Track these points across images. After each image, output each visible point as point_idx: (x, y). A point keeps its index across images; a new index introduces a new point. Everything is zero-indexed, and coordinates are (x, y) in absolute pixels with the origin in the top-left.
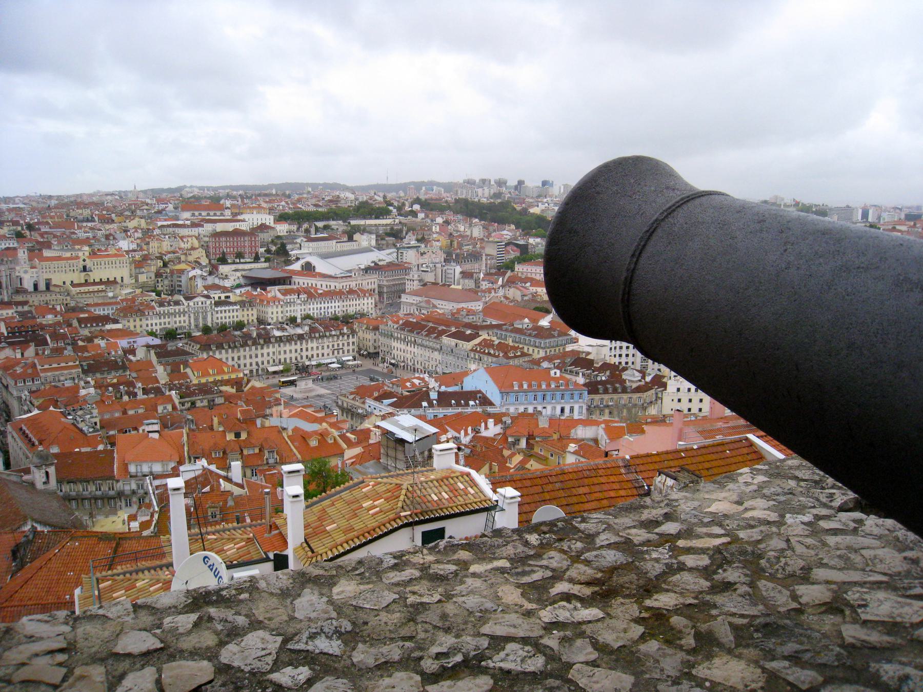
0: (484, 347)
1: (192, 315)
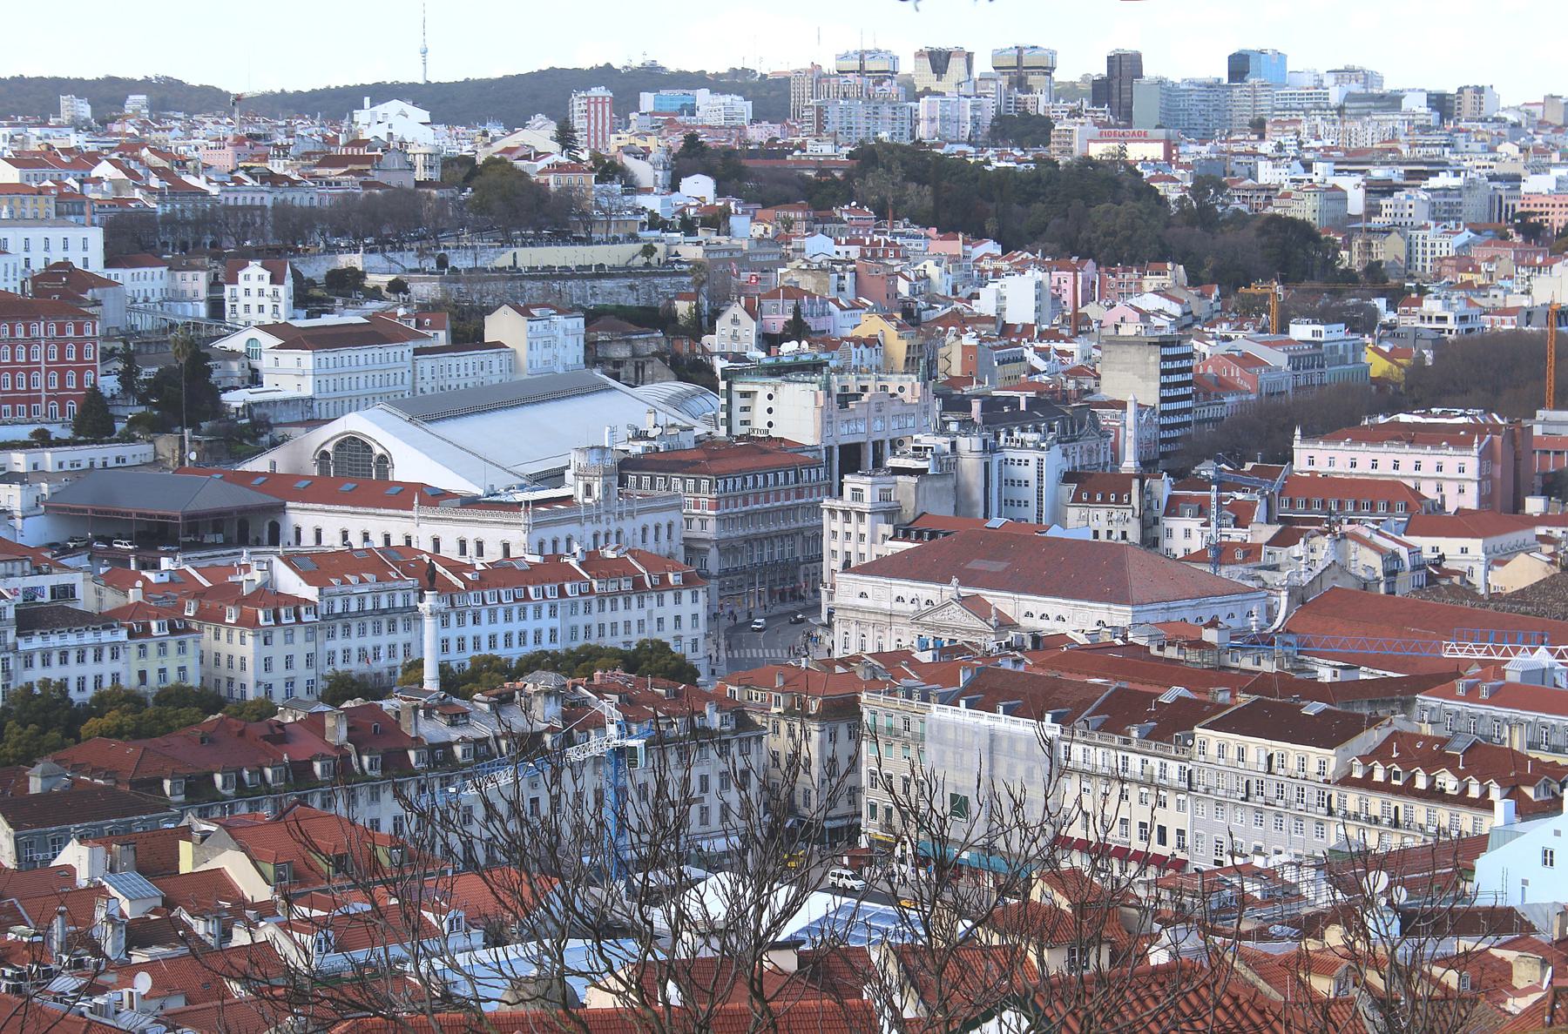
0: (1407, 762)
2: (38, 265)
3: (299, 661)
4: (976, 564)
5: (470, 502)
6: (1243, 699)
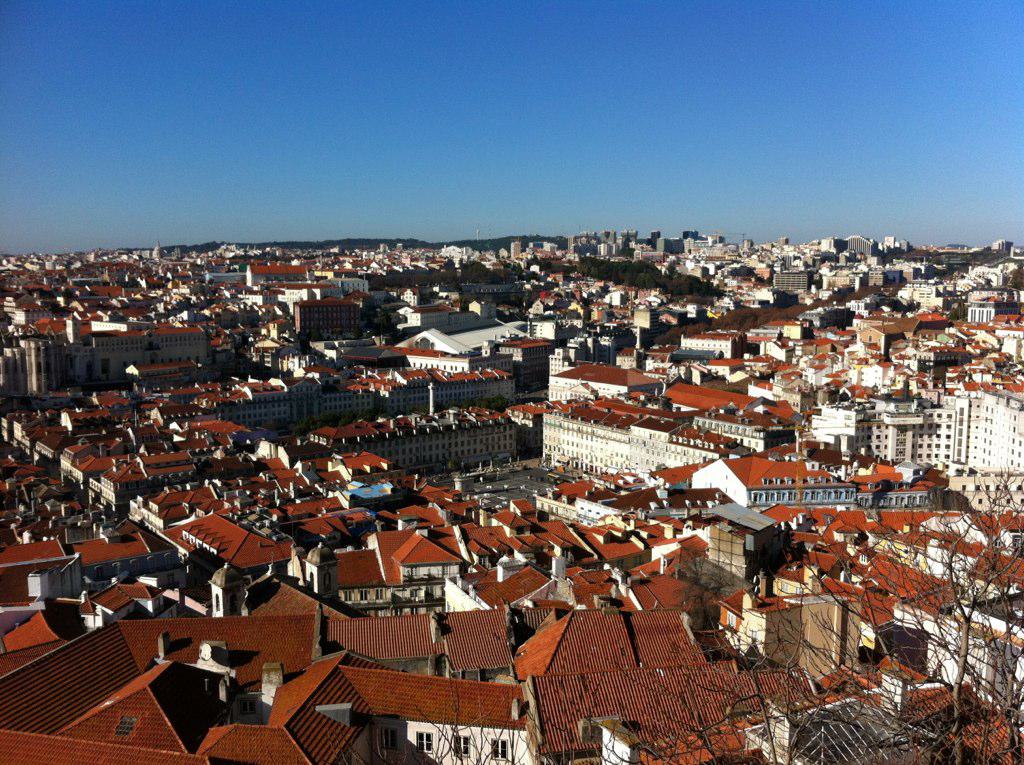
0: (688, 437)
1: (294, 405)
4: (587, 374)
5: (454, 356)
6: (648, 416)
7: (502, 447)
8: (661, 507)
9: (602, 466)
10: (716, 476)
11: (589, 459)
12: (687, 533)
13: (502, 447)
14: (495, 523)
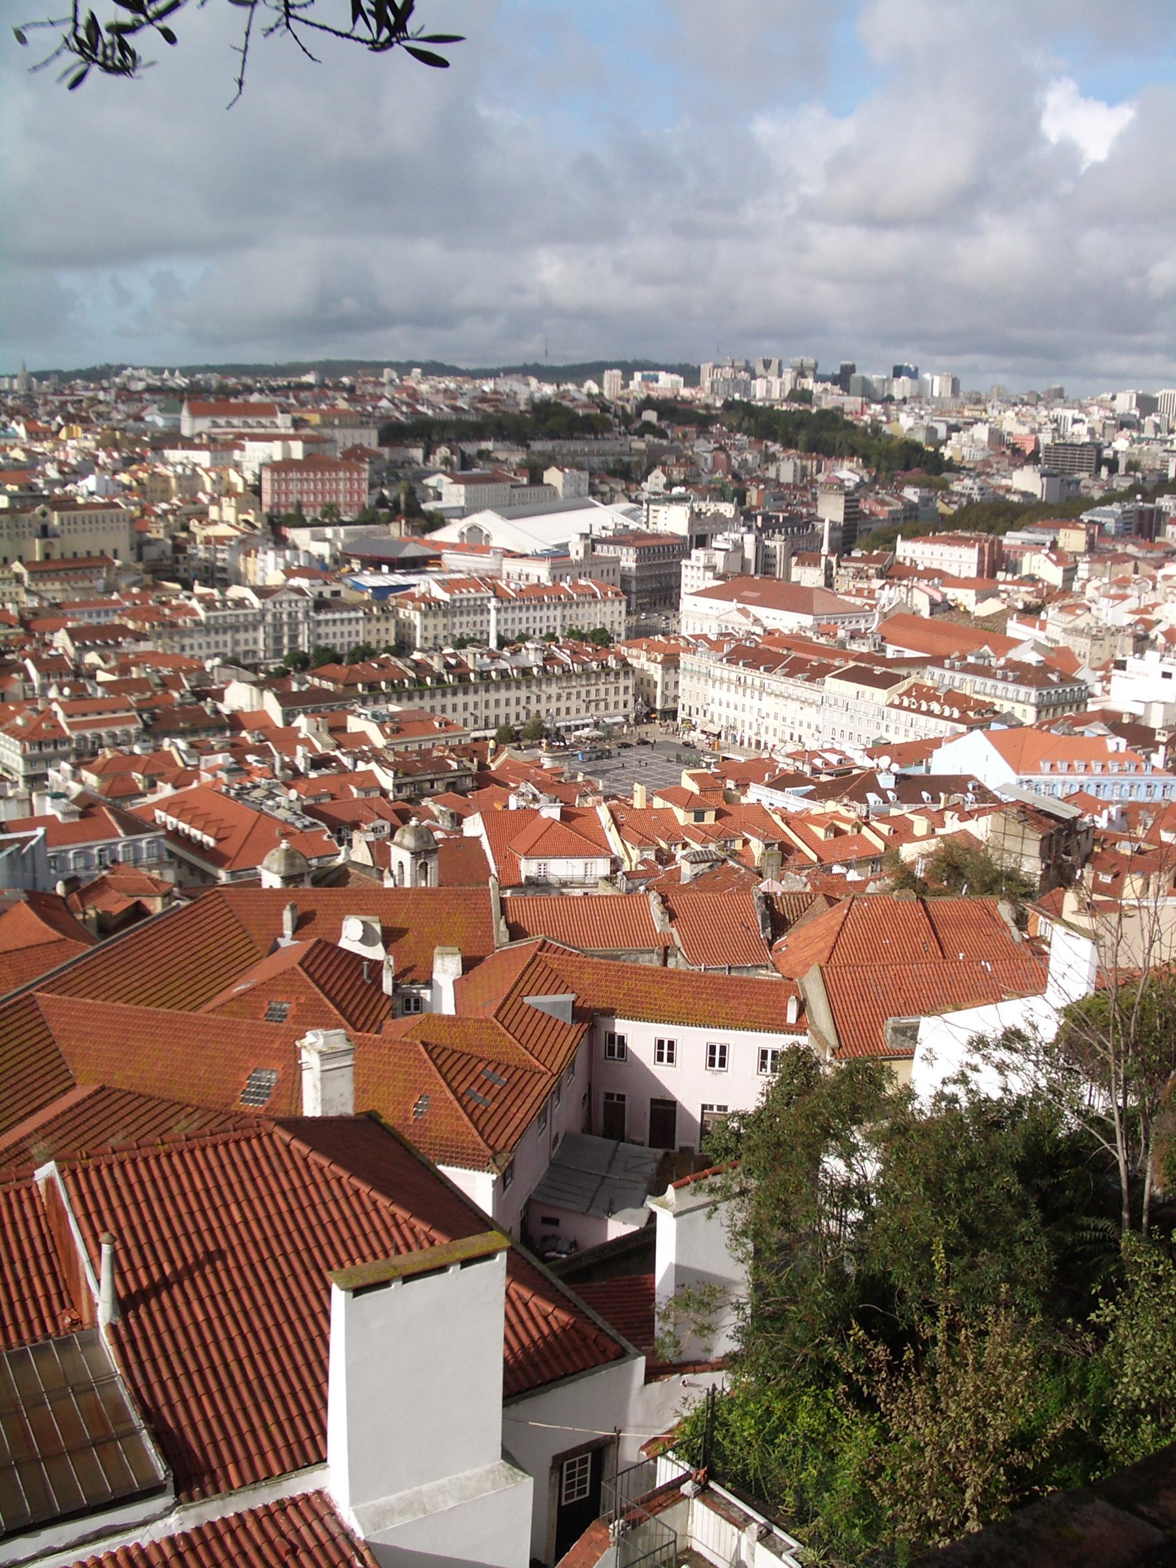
2: (349, 445)
3: (440, 627)
4: (746, 593)
6: (852, 664)
7: (612, 706)
8: (886, 800)
9: (777, 742)
10: (969, 755)
11: (755, 729)
12: (952, 825)
13: (612, 706)
14: (658, 803)
